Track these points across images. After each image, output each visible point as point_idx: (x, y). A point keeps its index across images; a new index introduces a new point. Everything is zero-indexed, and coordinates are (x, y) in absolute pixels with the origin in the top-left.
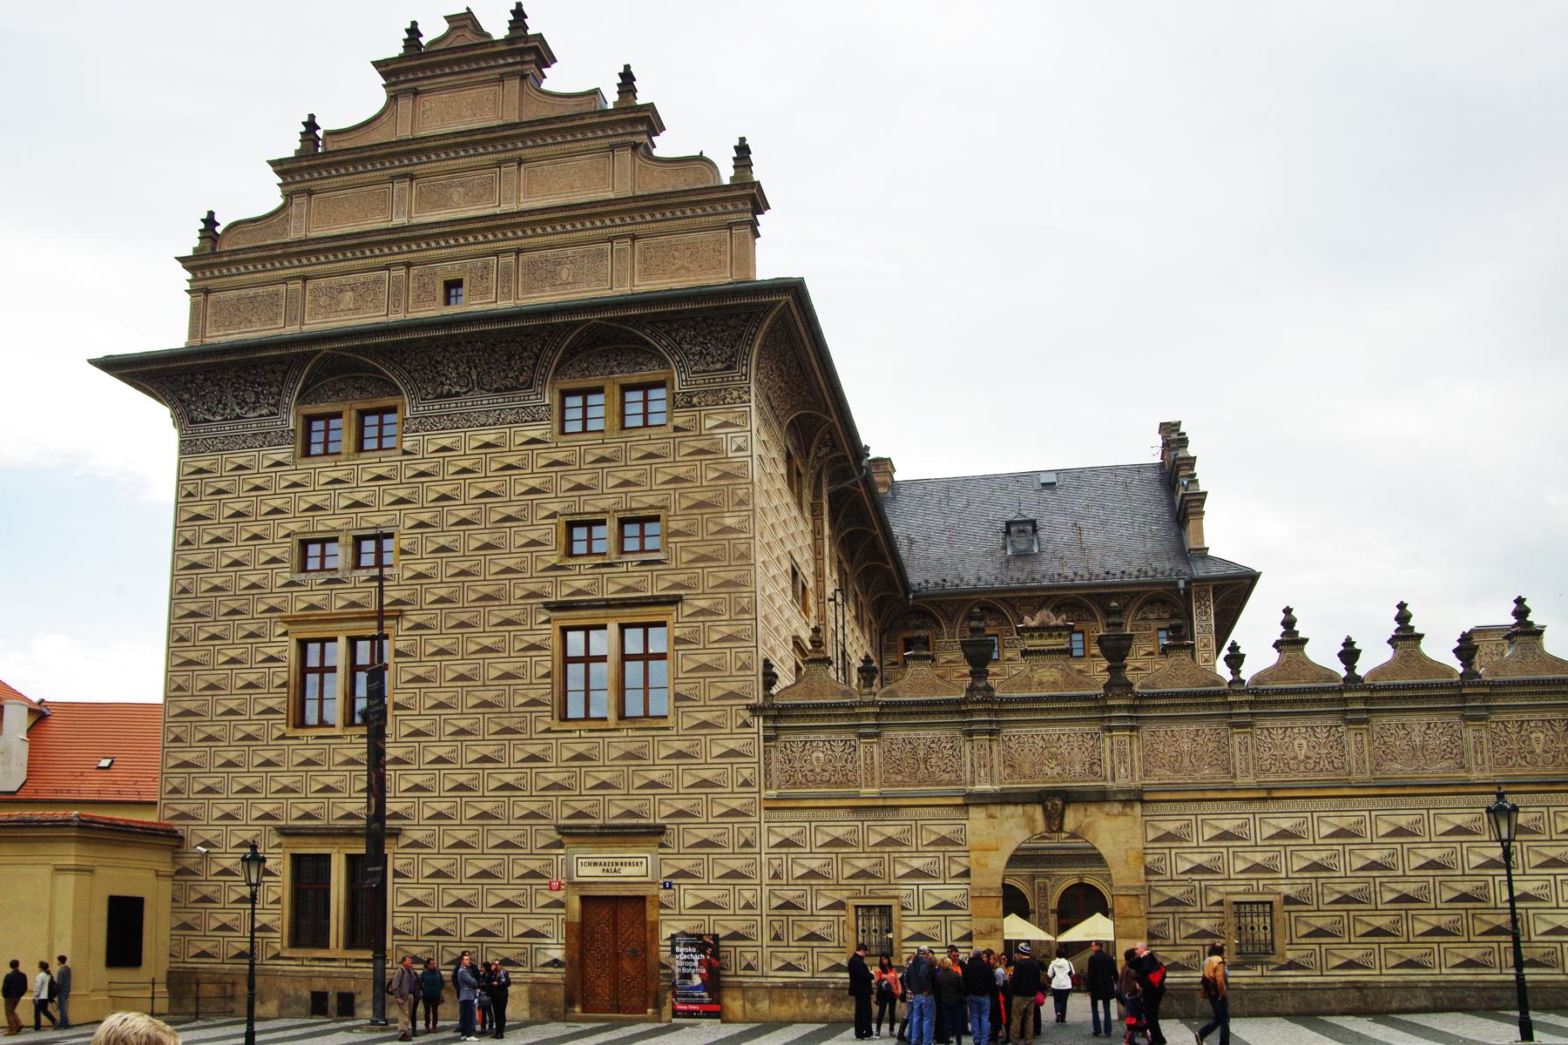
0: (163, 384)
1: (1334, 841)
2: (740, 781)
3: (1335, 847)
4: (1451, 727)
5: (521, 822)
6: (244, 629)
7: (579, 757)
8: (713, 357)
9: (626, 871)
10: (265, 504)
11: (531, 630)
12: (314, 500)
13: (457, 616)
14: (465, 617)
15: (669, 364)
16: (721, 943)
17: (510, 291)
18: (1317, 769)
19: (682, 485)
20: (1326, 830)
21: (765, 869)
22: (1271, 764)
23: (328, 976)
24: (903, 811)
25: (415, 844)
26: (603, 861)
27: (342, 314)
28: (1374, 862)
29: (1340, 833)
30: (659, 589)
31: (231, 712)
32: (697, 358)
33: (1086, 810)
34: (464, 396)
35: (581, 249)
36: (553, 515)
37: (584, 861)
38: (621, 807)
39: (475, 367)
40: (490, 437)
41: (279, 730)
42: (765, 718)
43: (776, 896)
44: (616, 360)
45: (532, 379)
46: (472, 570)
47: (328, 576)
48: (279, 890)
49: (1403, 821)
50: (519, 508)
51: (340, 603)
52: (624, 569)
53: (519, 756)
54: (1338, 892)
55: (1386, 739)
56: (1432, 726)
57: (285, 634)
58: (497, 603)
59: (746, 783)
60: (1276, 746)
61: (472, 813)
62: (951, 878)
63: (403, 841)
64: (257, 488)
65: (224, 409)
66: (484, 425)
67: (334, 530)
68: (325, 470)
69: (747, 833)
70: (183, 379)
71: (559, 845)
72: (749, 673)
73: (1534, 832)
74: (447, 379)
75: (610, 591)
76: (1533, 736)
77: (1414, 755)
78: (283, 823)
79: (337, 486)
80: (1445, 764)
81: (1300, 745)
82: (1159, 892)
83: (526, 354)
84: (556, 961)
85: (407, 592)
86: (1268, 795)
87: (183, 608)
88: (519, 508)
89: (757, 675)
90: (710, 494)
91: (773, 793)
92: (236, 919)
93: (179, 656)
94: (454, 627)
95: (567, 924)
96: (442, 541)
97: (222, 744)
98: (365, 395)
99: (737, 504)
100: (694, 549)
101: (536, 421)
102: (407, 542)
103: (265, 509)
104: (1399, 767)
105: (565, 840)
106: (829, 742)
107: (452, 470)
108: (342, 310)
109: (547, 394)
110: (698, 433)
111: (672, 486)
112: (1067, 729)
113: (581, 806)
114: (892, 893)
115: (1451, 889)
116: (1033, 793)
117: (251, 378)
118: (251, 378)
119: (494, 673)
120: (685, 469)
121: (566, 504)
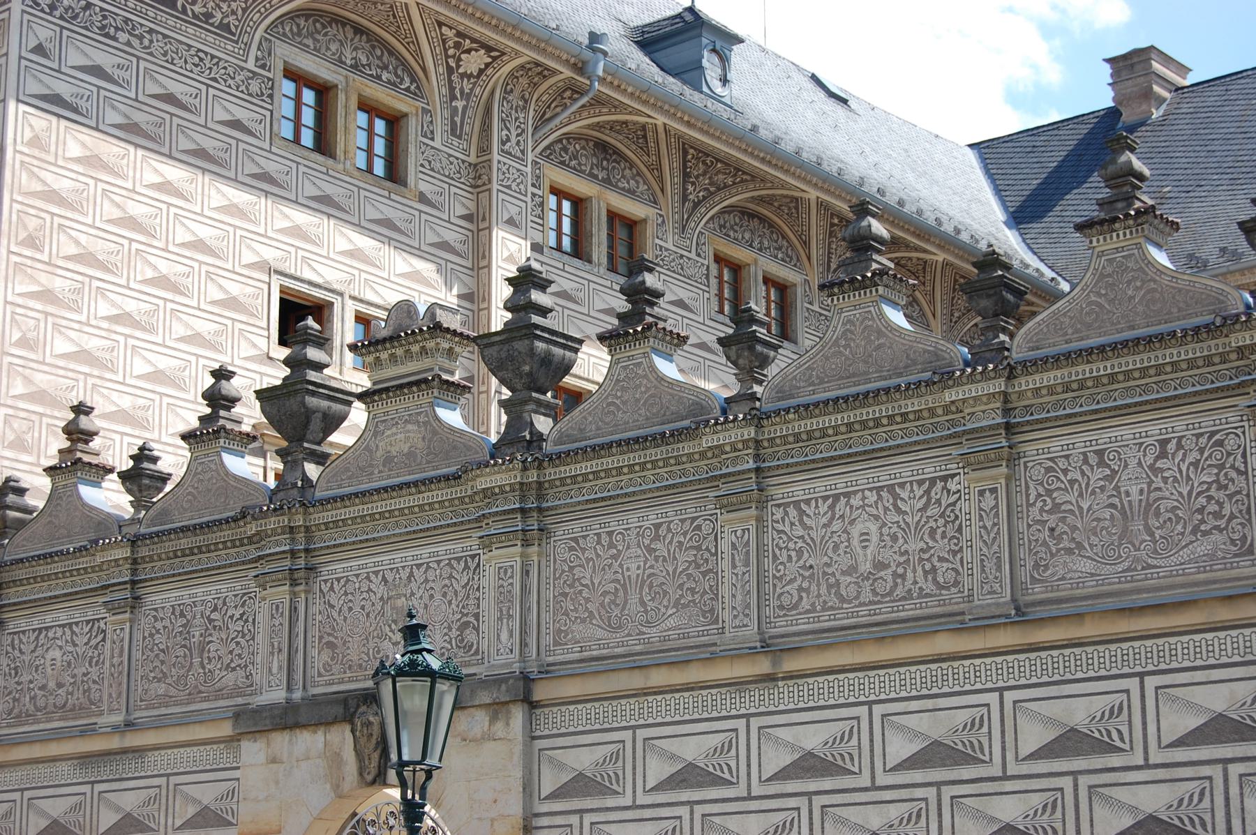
1: (917, 776)
3: (919, 793)
4: (1220, 443)
18: (899, 592)
20: (900, 749)
22: (800, 589)
24: (152, 757)
55: (1059, 497)
56: (1171, 447)
77: (1125, 530)
80: (1202, 547)
104: (1087, 566)
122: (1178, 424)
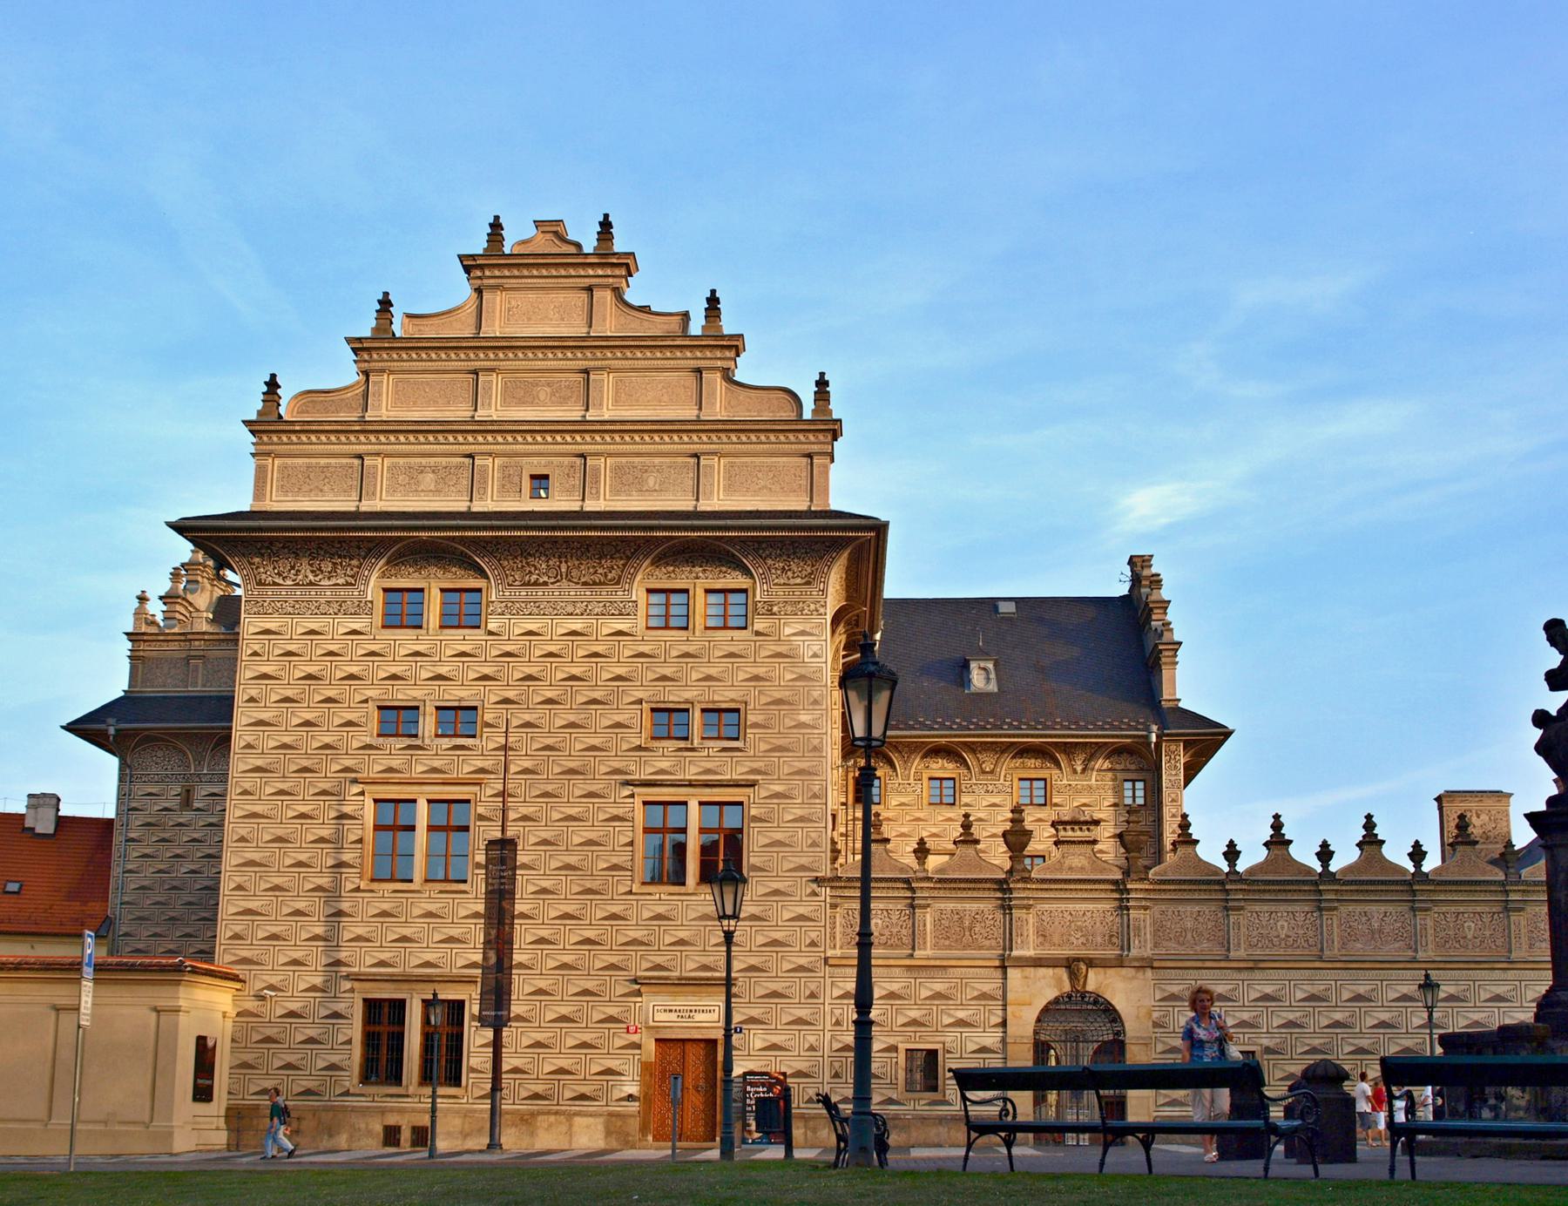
0: (236, 547)
2: (808, 942)
5: (601, 973)
6: (316, 786)
7: (658, 917)
8: (794, 573)
9: (699, 1017)
10: (341, 669)
11: (615, 803)
12: (393, 670)
13: (542, 786)
14: (549, 788)
15: (752, 575)
16: (788, 1080)
17: (598, 492)
18: (1295, 945)
19: (761, 683)
20: (1300, 995)
21: (828, 1017)
23: (401, 1111)
24: (951, 970)
26: (678, 1008)
28: (1338, 1021)
29: (1312, 998)
30: (736, 770)
31: (300, 864)
32: (779, 572)
33: (1105, 973)
34: (551, 586)
35: (667, 460)
36: (640, 702)
37: (659, 1008)
38: (698, 962)
39: (566, 562)
40: (577, 625)
41: (353, 882)
42: (832, 887)
43: (837, 1040)
44: (701, 566)
45: (620, 577)
46: (557, 746)
47: (408, 741)
48: (349, 1032)
49: (1362, 990)
50: (606, 693)
51: (420, 768)
52: (706, 754)
53: (600, 914)
54: (1308, 1045)
57: (362, 793)
58: (581, 777)
60: (1263, 927)
61: (552, 964)
62: (990, 1027)
64: (331, 653)
65: (296, 575)
66: (572, 614)
67: (415, 699)
68: (406, 640)
69: (813, 986)
70: (259, 545)
71: (639, 994)
72: (818, 849)
73: (1463, 1001)
74: (536, 569)
75: (691, 773)
76: (1466, 925)
77: (1373, 938)
78: (356, 970)
79: (419, 659)
80: (1397, 945)
81: (1282, 927)
82: (1164, 1043)
83: (618, 555)
84: (630, 1096)
85: (492, 762)
86: (1255, 965)
87: (246, 763)
88: (606, 693)
89: (826, 852)
90: (787, 693)
91: (838, 952)
92: (303, 1059)
93: (243, 809)
94: (538, 796)
95: (646, 1067)
96: (527, 717)
97: (291, 894)
98: (449, 575)
99: (812, 704)
100: (771, 740)
101: (620, 615)
102: (492, 715)
103: (340, 674)
105: (643, 989)
106: (887, 910)
107: (538, 653)
108: (422, 491)
109: (634, 592)
110: (777, 638)
111: (753, 684)
112: (1091, 906)
113: (659, 960)
114: (942, 1039)
115: (1397, 1044)
116: (1062, 959)
117: (334, 550)
118: (334, 550)
119: (577, 840)
120: (764, 669)
121: (651, 693)
122: (1390, 908)
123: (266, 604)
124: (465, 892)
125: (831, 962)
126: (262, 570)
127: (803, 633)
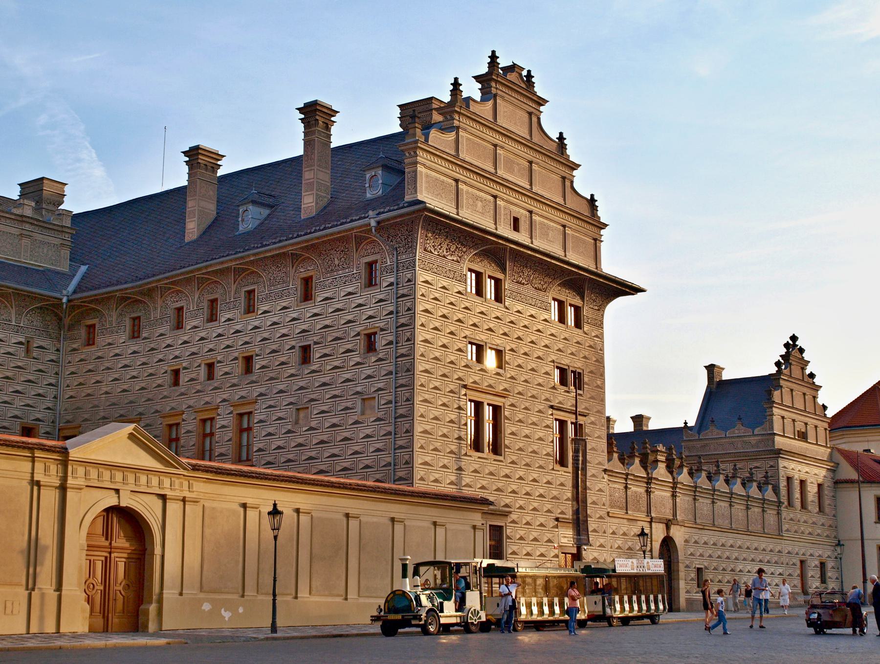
24: (639, 522)
25: (513, 522)
27: (478, 213)
36: (553, 361)
57: (465, 395)
59: (604, 505)
63: (510, 520)
65: (440, 249)
66: (531, 305)
67: (482, 341)
71: (557, 526)
79: (483, 316)
123: (426, 264)
124: (501, 461)
125: (610, 515)
126: (428, 242)
127: (596, 336)
